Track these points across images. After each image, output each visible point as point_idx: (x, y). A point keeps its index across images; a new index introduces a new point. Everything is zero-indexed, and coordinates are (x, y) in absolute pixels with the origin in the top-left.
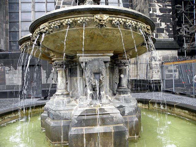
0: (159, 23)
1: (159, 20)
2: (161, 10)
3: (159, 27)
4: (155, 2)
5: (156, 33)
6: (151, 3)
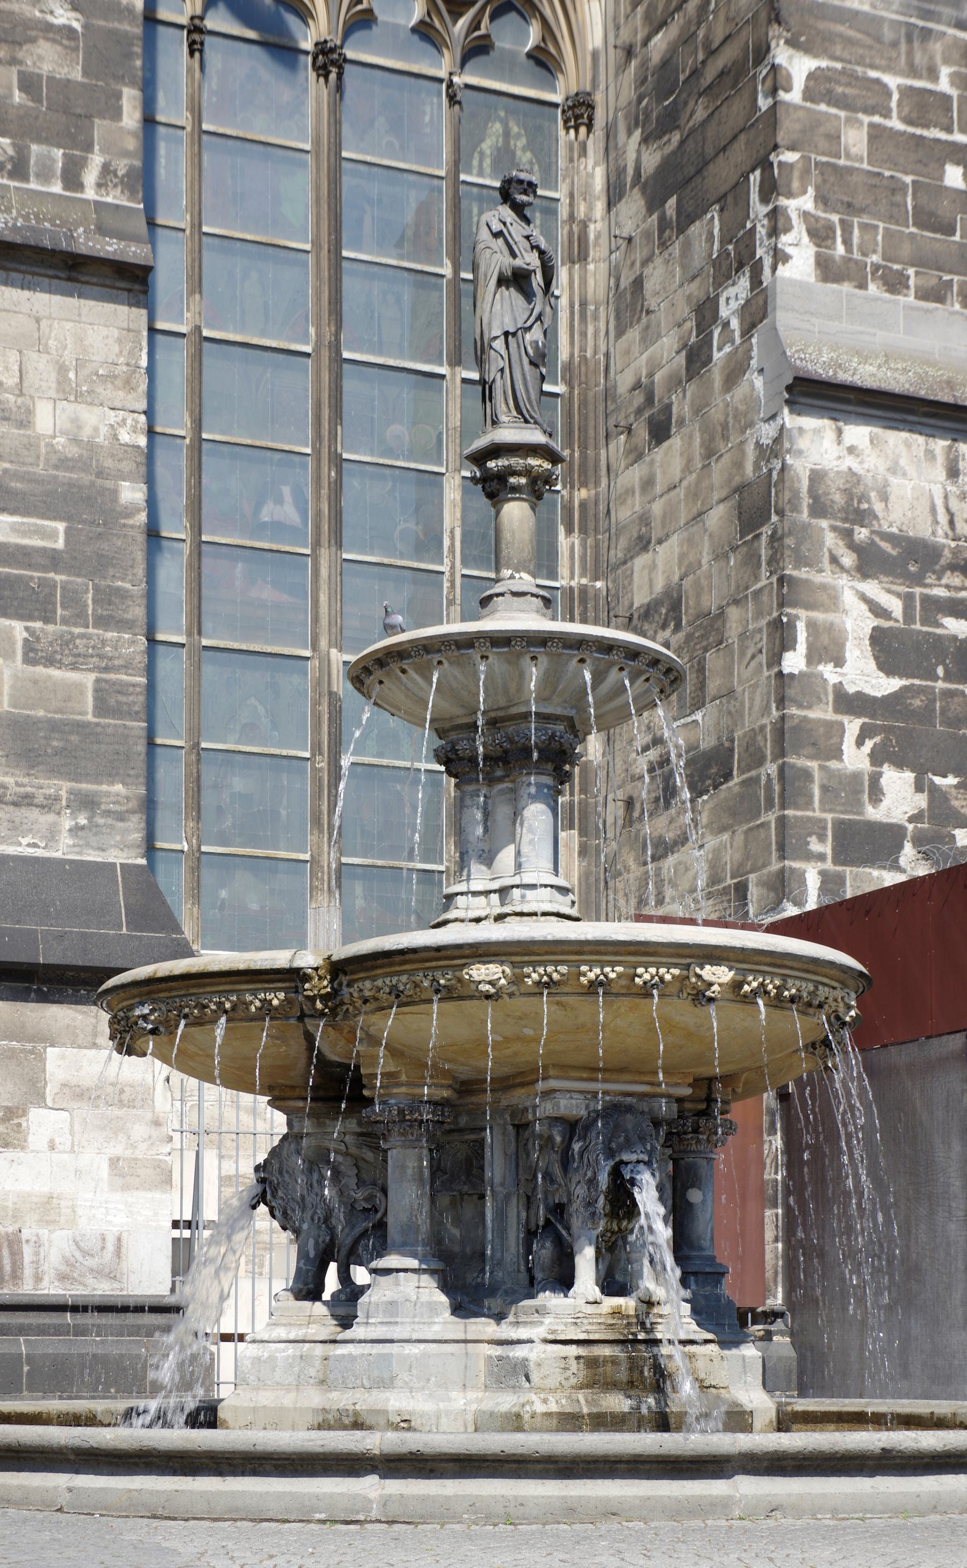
0: (856, 776)
1: (860, 742)
2: (888, 649)
3: (857, 806)
4: (834, 560)
5: (829, 865)
6: (803, 573)
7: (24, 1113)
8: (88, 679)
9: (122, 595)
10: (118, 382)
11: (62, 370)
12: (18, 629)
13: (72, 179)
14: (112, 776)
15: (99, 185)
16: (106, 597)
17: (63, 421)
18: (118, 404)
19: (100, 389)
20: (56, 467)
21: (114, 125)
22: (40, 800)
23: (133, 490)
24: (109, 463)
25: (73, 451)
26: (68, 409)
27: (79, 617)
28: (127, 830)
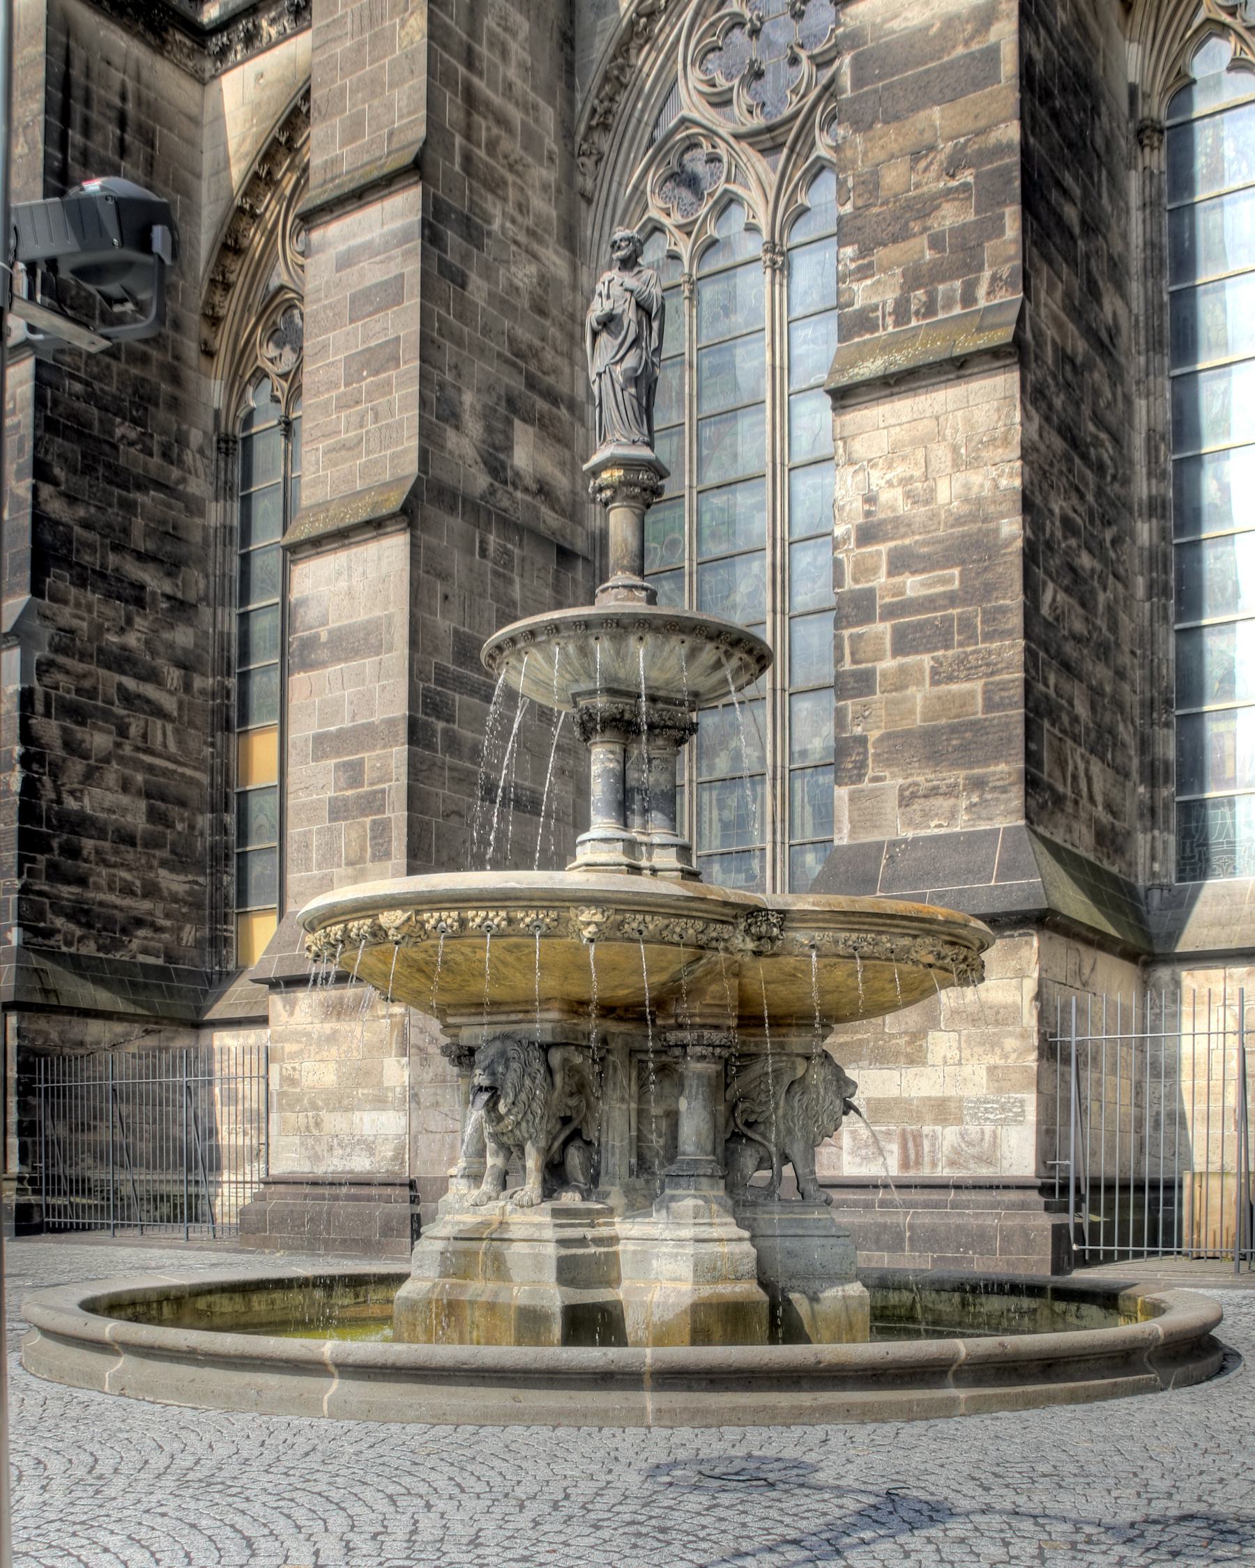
7: (925, 1036)
8: (977, 686)
9: (1003, 610)
10: (998, 443)
11: (955, 449)
12: (926, 660)
13: (968, 298)
14: (996, 758)
15: (989, 294)
16: (991, 616)
17: (957, 488)
18: (997, 460)
19: (984, 454)
20: (953, 526)
21: (999, 241)
22: (943, 789)
23: (1011, 524)
24: (992, 509)
25: (965, 509)
26: (960, 478)
27: (971, 638)
28: (1009, 800)
